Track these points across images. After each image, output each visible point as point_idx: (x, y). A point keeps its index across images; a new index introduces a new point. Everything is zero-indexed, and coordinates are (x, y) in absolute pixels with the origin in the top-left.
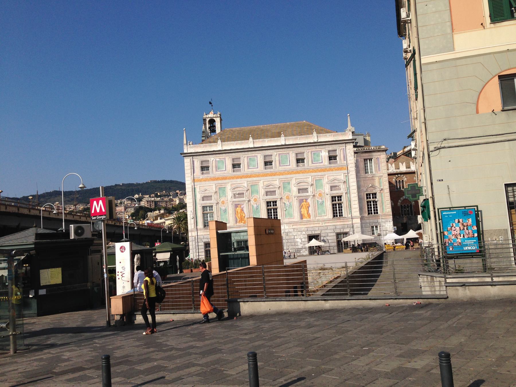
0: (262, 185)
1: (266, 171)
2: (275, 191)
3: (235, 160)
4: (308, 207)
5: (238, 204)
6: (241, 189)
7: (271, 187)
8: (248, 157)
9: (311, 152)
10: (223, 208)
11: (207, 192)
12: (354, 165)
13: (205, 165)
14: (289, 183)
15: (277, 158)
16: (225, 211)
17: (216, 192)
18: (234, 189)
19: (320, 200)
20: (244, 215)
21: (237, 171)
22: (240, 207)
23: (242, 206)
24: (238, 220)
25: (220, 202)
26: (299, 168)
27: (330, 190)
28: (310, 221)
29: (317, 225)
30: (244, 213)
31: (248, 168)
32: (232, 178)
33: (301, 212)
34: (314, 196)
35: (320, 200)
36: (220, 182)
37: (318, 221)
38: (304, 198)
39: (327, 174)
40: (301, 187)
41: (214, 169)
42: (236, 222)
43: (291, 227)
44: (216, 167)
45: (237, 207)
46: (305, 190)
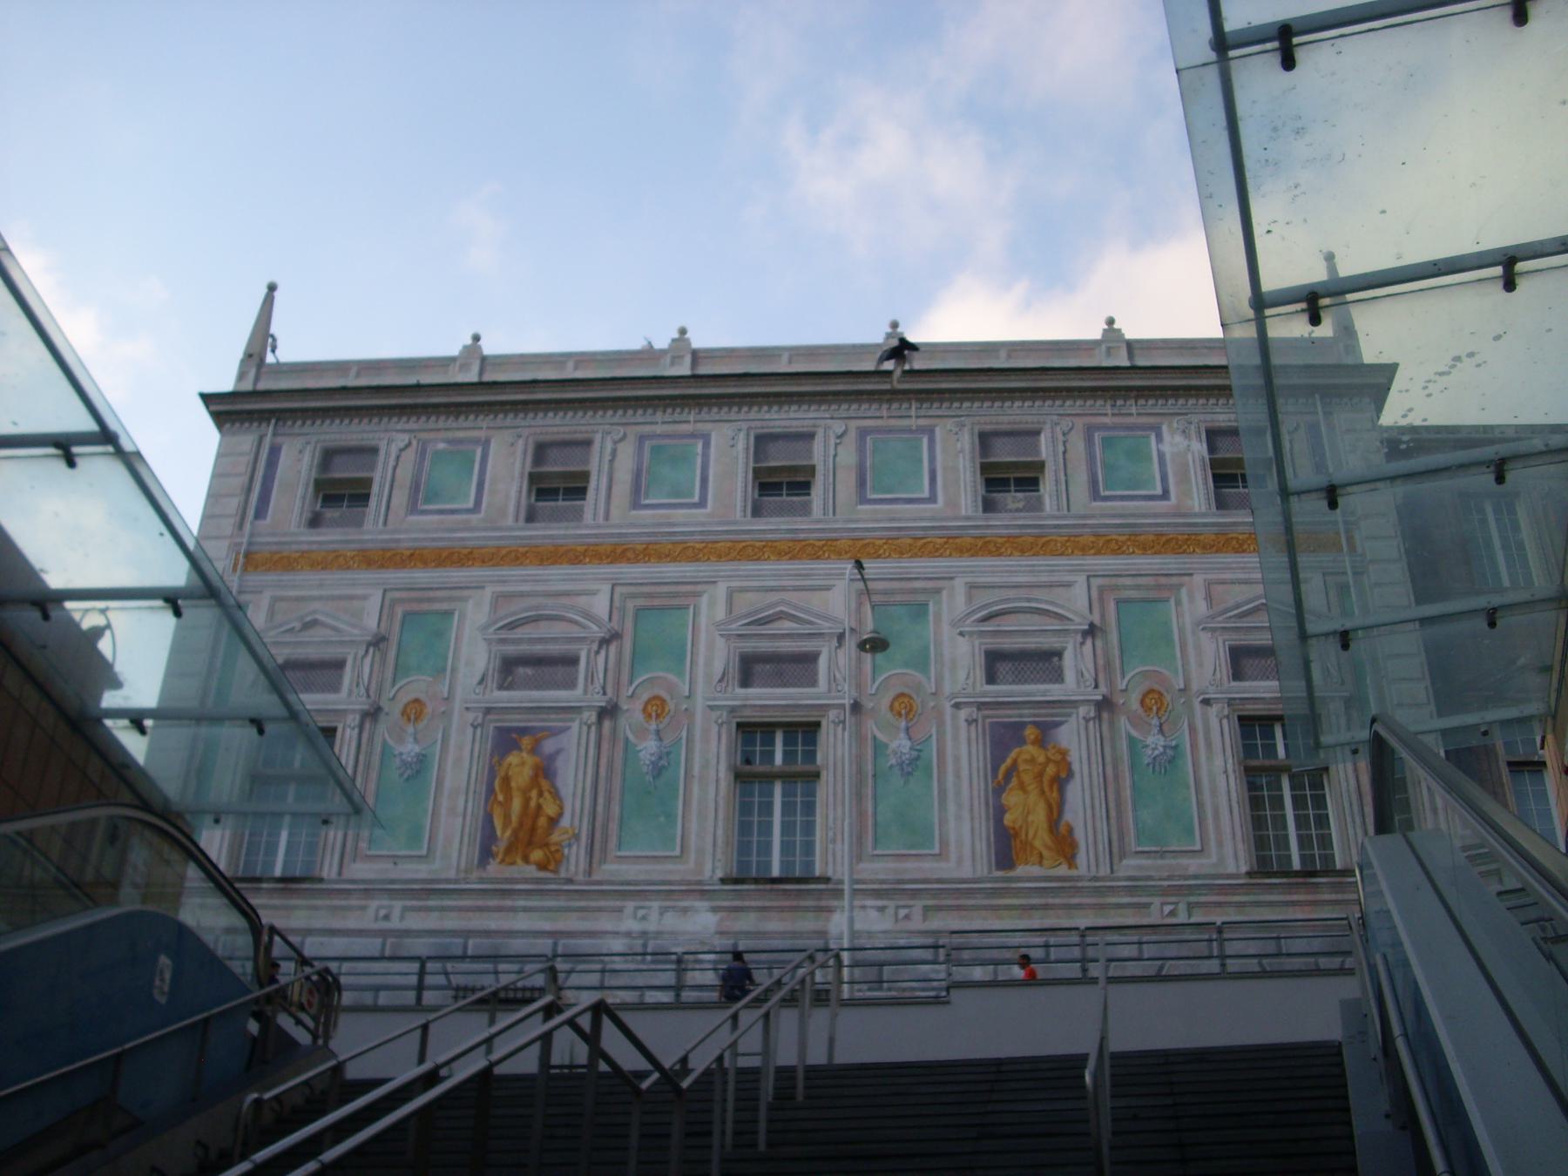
0: (721, 613)
1: (761, 525)
2: (810, 659)
3: (553, 454)
4: (1061, 782)
5: (523, 731)
6: (558, 629)
7: (787, 626)
8: (642, 438)
9: (1089, 431)
10: (409, 749)
11: (317, 634)
13: (343, 471)
14: (919, 611)
15: (847, 456)
16: (418, 768)
17: (378, 642)
18: (511, 626)
19: (1155, 741)
20: (550, 809)
21: (556, 517)
22: (534, 750)
23: (549, 746)
24: (504, 835)
25: (394, 710)
26: (997, 520)
27: (1225, 670)
28: (1069, 887)
30: (556, 795)
32: (515, 557)
33: (1000, 811)
35: (1155, 741)
36: (422, 576)
38: (1027, 715)
39: (1202, 570)
40: (1008, 644)
41: (400, 499)
42: (486, 854)
43: (917, 923)
44: (415, 487)
46: (1045, 662)
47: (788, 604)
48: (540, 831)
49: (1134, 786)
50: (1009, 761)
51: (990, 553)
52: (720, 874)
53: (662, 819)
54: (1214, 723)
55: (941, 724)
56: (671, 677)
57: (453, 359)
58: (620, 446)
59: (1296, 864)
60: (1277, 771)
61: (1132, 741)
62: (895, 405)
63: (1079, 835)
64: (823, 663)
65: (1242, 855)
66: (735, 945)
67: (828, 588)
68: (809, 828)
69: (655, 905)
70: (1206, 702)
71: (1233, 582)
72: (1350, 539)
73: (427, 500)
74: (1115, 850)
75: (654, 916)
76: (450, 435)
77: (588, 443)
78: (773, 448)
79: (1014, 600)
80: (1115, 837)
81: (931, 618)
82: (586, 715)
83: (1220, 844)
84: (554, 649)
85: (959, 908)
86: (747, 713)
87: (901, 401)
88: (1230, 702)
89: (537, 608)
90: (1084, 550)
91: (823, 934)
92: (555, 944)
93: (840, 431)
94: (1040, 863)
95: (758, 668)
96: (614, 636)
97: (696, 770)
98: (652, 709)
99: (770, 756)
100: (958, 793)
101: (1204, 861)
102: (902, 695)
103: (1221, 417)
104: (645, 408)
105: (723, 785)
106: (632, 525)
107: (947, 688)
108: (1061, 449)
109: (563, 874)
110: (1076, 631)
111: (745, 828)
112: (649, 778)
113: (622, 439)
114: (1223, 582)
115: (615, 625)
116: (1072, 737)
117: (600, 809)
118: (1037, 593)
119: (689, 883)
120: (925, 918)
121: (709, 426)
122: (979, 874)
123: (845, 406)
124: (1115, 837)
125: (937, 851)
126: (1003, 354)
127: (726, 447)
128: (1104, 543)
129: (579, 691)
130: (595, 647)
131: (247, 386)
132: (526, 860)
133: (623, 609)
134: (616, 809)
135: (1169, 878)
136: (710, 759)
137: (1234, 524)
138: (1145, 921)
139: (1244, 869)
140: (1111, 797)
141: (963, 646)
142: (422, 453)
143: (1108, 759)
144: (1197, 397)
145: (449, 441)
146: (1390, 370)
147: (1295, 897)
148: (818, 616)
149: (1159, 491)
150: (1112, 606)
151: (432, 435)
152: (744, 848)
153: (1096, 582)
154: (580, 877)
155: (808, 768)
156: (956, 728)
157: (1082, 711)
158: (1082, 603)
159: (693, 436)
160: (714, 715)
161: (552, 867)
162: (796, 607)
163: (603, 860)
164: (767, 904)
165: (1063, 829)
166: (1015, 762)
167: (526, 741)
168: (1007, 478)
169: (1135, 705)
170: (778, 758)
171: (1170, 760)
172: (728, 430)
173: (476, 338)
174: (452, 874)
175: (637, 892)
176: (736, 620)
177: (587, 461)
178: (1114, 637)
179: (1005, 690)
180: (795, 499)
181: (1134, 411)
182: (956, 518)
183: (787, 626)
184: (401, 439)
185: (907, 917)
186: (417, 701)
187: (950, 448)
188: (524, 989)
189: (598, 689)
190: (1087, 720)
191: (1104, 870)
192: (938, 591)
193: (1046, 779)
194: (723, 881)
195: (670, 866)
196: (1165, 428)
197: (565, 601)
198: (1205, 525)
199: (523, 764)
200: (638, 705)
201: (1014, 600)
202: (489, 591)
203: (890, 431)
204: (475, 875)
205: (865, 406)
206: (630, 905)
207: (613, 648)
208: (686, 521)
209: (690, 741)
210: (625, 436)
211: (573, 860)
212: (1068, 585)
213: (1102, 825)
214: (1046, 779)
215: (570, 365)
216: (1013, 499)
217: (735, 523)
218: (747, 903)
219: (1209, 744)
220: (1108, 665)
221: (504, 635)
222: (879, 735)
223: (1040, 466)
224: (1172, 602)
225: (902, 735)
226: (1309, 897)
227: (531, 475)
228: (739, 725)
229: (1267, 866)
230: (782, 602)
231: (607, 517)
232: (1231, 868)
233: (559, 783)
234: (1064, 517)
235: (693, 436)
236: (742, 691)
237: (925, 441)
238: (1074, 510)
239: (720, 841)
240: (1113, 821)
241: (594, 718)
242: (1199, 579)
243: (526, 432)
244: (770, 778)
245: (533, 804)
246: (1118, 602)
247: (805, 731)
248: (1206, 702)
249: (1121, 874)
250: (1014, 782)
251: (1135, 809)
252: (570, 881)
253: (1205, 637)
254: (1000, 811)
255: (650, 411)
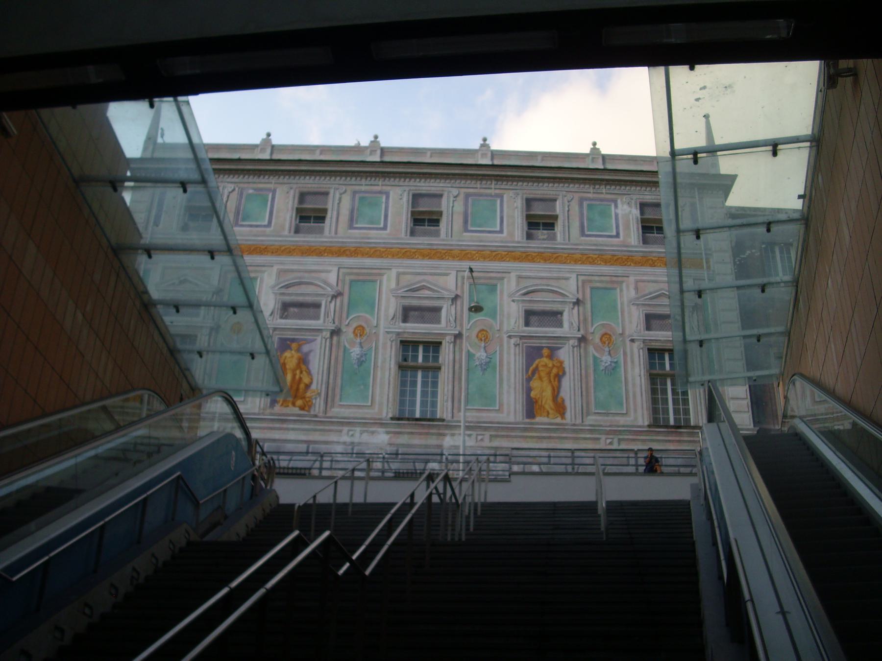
0: (393, 285)
2: (438, 310)
3: (309, 198)
4: (559, 377)
7: (427, 293)
8: (355, 193)
9: (581, 201)
12: (728, 256)
14: (493, 288)
15: (459, 207)
19: (606, 359)
20: (306, 380)
21: (310, 231)
22: (298, 350)
23: (306, 348)
26: (533, 244)
27: (642, 326)
28: (561, 428)
29: (590, 446)
30: (309, 373)
31: (351, 227)
32: (288, 251)
33: (529, 390)
34: (583, 340)
35: (606, 359)
37: (594, 430)
38: (544, 343)
39: (634, 274)
43: (487, 443)
44: (237, 213)
45: (289, 347)
46: (553, 317)
47: (428, 282)
48: (301, 391)
49: (595, 381)
50: (534, 366)
51: (530, 261)
52: (390, 415)
53: (362, 387)
54: (636, 351)
55: (501, 346)
56: (368, 316)
57: (256, 146)
58: (343, 196)
59: (672, 422)
60: (664, 376)
61: (595, 358)
62: (484, 182)
63: (567, 403)
64: (444, 312)
65: (646, 416)
66: (397, 450)
67: (447, 275)
68: (435, 394)
69: (358, 429)
70: (632, 341)
71: (649, 281)
72: (707, 262)
73: (243, 220)
74: (584, 411)
75: (357, 435)
76: (255, 186)
77: (326, 194)
78: (422, 201)
79: (541, 285)
80: (585, 405)
81: (498, 292)
82: (324, 333)
83: (635, 411)
84: (309, 299)
85: (507, 436)
86: (406, 336)
87: (487, 180)
88: (644, 341)
89: (300, 278)
90: (576, 261)
91: (440, 446)
92: (308, 447)
93: (455, 194)
94: (548, 416)
95: (412, 313)
96: (339, 294)
97: (379, 364)
98: (358, 332)
99: (415, 358)
100: (509, 380)
101: (628, 419)
102: (483, 330)
103: (648, 197)
104: (356, 177)
105: (393, 371)
106: (349, 238)
107: (505, 328)
108: (567, 209)
109: (312, 413)
110: (570, 302)
111: (403, 393)
112: (356, 366)
113: (345, 192)
114: (644, 281)
115: (339, 288)
116: (565, 355)
117: (331, 381)
118: (551, 282)
119: (375, 419)
120: (491, 441)
121: (389, 188)
122: (518, 420)
123: (458, 181)
124: (585, 405)
125: (497, 408)
126: (539, 158)
127: (397, 200)
128: (586, 258)
129: (321, 321)
130: (329, 299)
131: (148, 155)
132: (294, 404)
133: (344, 281)
134: (339, 381)
135: (610, 426)
136: (387, 358)
137: (650, 252)
138: (598, 447)
139: (646, 423)
140: (584, 386)
141: (514, 306)
142: (241, 194)
143: (583, 366)
144: (636, 186)
145: (255, 189)
146: (732, 178)
147: (670, 438)
148: (443, 289)
149: (614, 233)
150: (588, 291)
151: (246, 185)
152: (402, 403)
153: (581, 278)
154: (321, 414)
155: (436, 364)
156: (509, 348)
157: (571, 342)
158: (573, 288)
159: (380, 192)
160: (389, 336)
161: (307, 408)
162: (431, 283)
163: (333, 406)
164: (413, 431)
165: (559, 400)
166: (537, 368)
167: (294, 345)
168: (539, 222)
169: (597, 340)
170: (420, 359)
171: (613, 368)
172: (399, 190)
173: (269, 135)
174: (257, 411)
175: (349, 423)
176: (400, 289)
177: (326, 203)
178: (588, 306)
179: (533, 330)
180: (432, 228)
181: (604, 191)
182: (513, 242)
183: (427, 293)
184: (230, 187)
185: (482, 440)
186: (238, 323)
187: (510, 207)
188: (292, 468)
189: (331, 320)
190: (573, 347)
191: (579, 421)
192: (503, 279)
193: (552, 375)
194: (392, 419)
195: (366, 411)
196: (619, 201)
197: (313, 275)
198: (636, 252)
199: (292, 357)
200: (351, 330)
201: (541, 285)
202: (275, 268)
203: (481, 195)
204: (268, 411)
205: (469, 182)
206: (346, 429)
207: (338, 300)
208: (377, 237)
209: (376, 348)
210: (345, 192)
211: (317, 406)
212: (567, 279)
213: (578, 399)
214: (552, 375)
215: (318, 152)
216: (542, 233)
217: (402, 239)
218: (403, 430)
219: (633, 362)
220: (585, 320)
221: (283, 291)
222: (471, 350)
223: (556, 217)
224: (618, 290)
225: (482, 350)
226: (678, 438)
227: (297, 209)
228: (401, 342)
229: (657, 423)
230: (424, 281)
231: (336, 233)
232: (640, 423)
233: (311, 367)
234: (566, 244)
235: (380, 192)
236: (403, 325)
237: (499, 202)
238: (572, 241)
239: (391, 399)
240: (584, 398)
241: (328, 335)
242: (632, 279)
243: (295, 186)
244: (415, 369)
245: (297, 377)
246: (592, 288)
247: (433, 346)
248: (632, 341)
249: (587, 423)
250: (536, 376)
251: (595, 392)
252: (316, 416)
253: (634, 308)
254: (529, 390)
255: (359, 179)
